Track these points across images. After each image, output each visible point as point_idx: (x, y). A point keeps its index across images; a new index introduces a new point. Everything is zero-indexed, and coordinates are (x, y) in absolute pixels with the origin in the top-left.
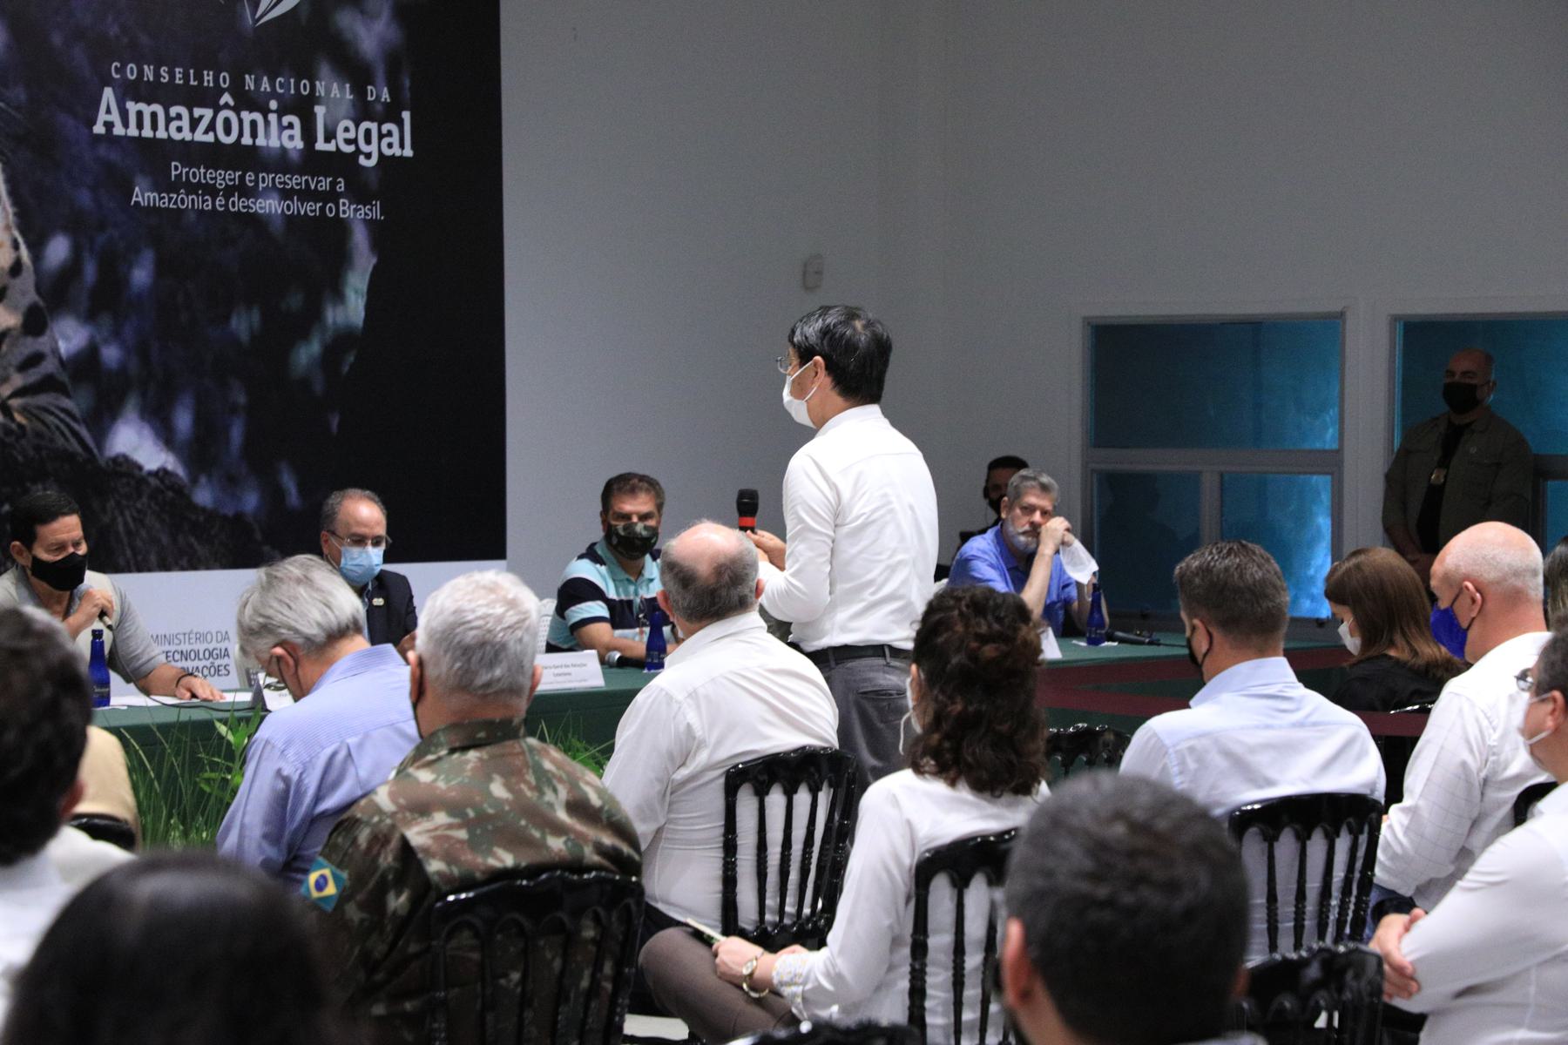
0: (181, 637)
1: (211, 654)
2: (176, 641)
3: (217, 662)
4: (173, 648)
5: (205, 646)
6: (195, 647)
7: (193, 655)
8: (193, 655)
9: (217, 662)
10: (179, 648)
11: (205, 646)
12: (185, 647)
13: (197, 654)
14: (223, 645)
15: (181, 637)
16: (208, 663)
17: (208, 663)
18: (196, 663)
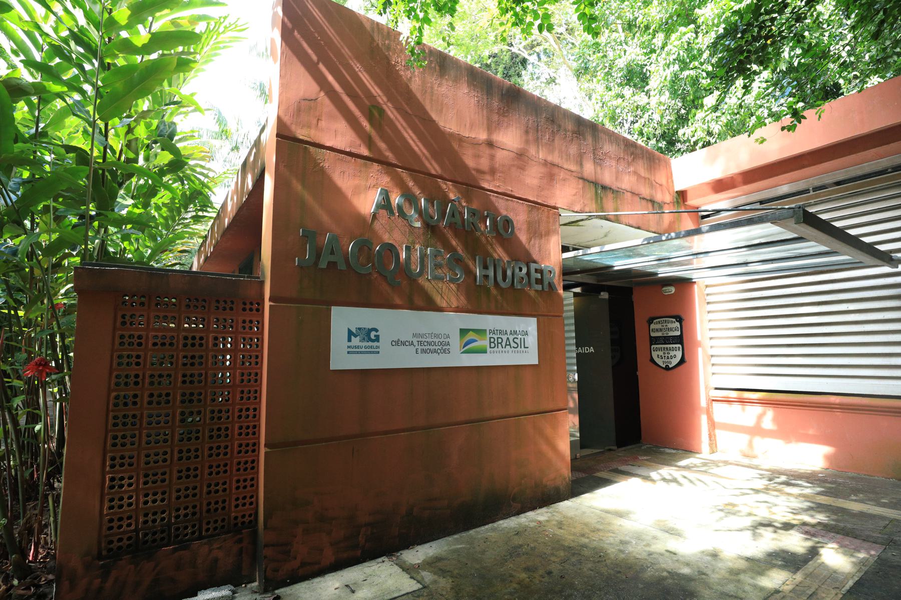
0: (427, 335)
1: (441, 344)
2: (425, 337)
3: (444, 348)
4: (424, 340)
5: (439, 340)
6: (434, 340)
7: (433, 343)
8: (433, 343)
9: (444, 348)
10: (426, 340)
11: (440, 340)
12: (429, 340)
13: (435, 343)
14: (447, 340)
15: (427, 335)
16: (440, 348)
17: (440, 348)
18: (434, 347)
